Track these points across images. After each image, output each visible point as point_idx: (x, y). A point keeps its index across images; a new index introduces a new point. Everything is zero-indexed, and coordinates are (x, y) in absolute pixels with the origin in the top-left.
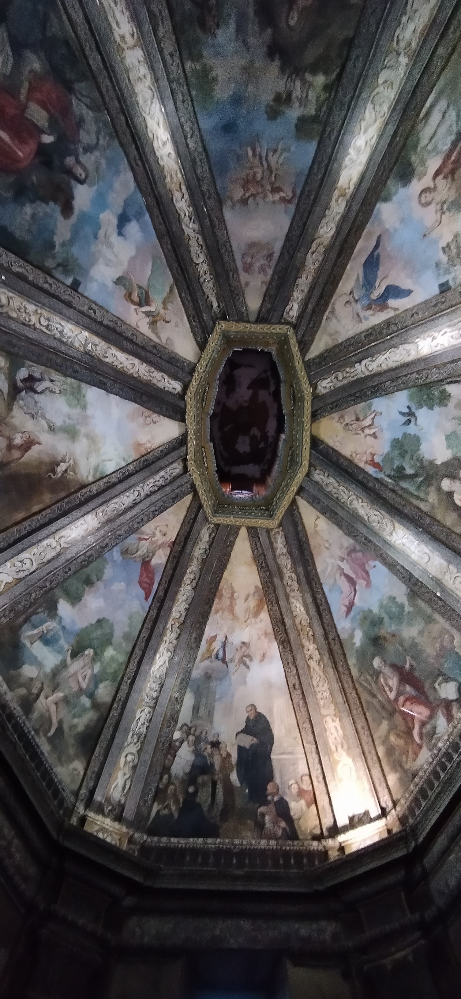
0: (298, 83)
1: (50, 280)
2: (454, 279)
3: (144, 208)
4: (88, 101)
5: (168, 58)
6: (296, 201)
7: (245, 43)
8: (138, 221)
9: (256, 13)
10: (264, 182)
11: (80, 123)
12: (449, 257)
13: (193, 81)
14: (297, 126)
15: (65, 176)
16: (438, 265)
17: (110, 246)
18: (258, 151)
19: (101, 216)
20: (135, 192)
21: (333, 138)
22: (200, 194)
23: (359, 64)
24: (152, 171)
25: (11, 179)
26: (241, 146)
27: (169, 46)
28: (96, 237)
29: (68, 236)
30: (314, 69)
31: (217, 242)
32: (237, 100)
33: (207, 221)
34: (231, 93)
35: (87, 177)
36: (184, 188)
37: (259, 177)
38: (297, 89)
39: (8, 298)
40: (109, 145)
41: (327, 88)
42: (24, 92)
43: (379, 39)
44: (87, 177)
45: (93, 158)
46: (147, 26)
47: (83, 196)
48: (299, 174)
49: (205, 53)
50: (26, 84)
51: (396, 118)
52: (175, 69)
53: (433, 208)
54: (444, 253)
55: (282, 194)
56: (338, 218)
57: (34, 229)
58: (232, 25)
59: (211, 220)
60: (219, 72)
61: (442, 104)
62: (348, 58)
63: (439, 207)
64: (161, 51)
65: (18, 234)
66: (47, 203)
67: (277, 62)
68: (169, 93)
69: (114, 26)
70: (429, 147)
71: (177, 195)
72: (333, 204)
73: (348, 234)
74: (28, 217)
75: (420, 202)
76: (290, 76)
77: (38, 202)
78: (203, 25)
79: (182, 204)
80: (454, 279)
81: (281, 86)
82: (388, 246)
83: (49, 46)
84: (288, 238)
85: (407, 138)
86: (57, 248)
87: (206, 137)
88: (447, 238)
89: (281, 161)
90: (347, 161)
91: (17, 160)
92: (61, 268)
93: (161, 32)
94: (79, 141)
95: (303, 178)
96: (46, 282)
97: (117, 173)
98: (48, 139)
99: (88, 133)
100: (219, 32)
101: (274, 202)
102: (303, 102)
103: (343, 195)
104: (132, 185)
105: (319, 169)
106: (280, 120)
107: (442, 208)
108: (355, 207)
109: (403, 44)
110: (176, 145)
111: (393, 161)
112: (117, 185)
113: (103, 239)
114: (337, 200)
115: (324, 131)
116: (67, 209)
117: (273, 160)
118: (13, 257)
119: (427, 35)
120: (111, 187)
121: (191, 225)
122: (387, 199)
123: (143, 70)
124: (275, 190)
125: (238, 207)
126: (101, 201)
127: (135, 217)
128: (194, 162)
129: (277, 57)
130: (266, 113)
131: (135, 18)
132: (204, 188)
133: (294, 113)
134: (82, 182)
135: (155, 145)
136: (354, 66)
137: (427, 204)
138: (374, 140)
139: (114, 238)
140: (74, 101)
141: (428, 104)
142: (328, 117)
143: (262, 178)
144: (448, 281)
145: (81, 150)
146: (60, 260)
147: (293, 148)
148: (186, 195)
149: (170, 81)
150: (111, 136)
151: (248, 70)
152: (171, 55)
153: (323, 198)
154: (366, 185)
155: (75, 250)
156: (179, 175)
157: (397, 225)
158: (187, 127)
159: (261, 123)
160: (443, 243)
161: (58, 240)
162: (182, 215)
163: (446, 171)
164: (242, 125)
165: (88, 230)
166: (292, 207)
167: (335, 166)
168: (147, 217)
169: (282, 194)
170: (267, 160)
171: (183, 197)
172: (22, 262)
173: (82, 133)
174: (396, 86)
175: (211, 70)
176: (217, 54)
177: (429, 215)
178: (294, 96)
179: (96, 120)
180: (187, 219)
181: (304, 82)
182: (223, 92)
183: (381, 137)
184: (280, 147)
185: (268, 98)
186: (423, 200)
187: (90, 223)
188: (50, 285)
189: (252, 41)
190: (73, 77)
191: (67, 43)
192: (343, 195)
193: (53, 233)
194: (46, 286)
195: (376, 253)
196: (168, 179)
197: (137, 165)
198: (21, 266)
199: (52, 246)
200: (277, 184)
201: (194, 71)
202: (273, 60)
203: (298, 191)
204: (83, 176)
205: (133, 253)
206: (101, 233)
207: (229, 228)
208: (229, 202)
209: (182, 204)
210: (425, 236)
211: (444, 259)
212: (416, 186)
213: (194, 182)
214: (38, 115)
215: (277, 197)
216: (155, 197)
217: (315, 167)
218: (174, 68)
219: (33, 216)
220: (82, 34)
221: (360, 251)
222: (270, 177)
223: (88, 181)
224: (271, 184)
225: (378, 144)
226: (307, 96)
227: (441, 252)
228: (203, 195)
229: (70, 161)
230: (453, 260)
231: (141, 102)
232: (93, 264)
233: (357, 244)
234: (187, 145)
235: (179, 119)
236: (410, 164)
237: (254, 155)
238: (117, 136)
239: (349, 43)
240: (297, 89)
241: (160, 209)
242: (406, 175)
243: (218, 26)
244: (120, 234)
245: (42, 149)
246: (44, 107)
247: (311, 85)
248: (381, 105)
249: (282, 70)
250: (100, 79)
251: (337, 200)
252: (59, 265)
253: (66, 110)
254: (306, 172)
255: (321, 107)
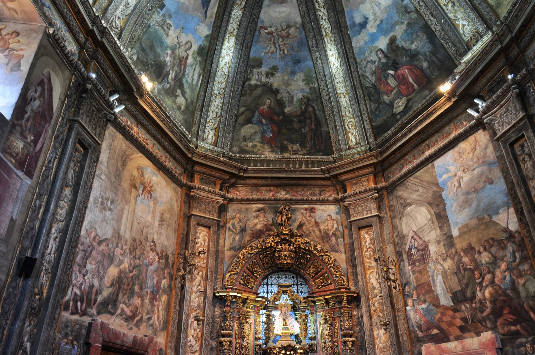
0: (263, 80)
1: (418, 6)
2: (159, 13)
3: (349, 28)
4: (367, 79)
5: (325, 88)
6: (258, 28)
7: (289, 94)
8: (354, 22)
9: (285, 103)
10: (277, 37)
11: (373, 73)
12: (167, 23)
13: (314, 80)
14: (262, 64)
15: (388, 55)
16: (170, 17)
17: (374, 14)
18: (281, 53)
19: (375, 31)
20: (353, 37)
21: (242, 59)
22: (315, 32)
23: (236, 89)
24: (341, 45)
25: (416, 63)
26: (291, 54)
27: (324, 93)
28: (382, 21)
29: (397, 27)
30: (256, 86)
31: (306, 4)
32: (293, 73)
33: (312, 17)
34: (296, 76)
35: (377, 51)
36: (324, 34)
37: (281, 40)
38: (264, 79)
39: (447, 5)
40: (362, 60)
41: (249, 79)
42: (395, 91)
43: (230, 98)
44: (377, 51)
45: (372, 58)
46: (333, 100)
47: (383, 43)
48: (257, 42)
49: (308, 90)
50: (392, 93)
51: (213, 72)
52: (323, 84)
53: (184, 42)
54: (170, 24)
55: (266, 31)
56: (231, 21)
57: (414, 36)
58: (295, 99)
59: (309, 17)
60: (301, 84)
61: (194, 82)
62: (242, 90)
63: (181, 44)
64: (328, 91)
65: (424, 37)
66: (403, 46)
67: (274, 88)
68: (327, 77)
69: (348, 101)
70: (194, 65)
71: (328, 31)
72: (236, 28)
73: (223, 16)
74: (415, 43)
75: (191, 42)
76: (268, 83)
77: (407, 48)
78: (308, 99)
79: (326, 26)
80: (159, 13)
81: (272, 80)
82: (200, 15)
83: (379, 101)
84: (260, 7)
85: (205, 65)
86: (406, 22)
87: (310, 58)
88: (171, 32)
89: (269, 48)
90: (232, 49)
91: (409, 69)
92: (409, 10)
93: (327, 97)
94: (376, 67)
95: (255, 39)
96: (420, 6)
97: (360, 48)
98: (392, 72)
99: (371, 68)
100: (301, 97)
101: (271, 27)
102: (260, 74)
103: (230, 33)
104: (354, 40)
105: (247, 45)
106: (271, 66)
107: (179, 44)
108: (223, 28)
109: (219, 97)
110: (326, 55)
111: (209, 54)
112: (362, 42)
113: (378, 19)
114: (234, 30)
115: (247, 62)
116: (393, 41)
117: (273, 48)
118: (433, 27)
119: (210, 102)
120: (366, 43)
121: (322, 14)
122: (207, 36)
123: (338, 85)
124: (271, 33)
125: (292, 24)
126: (373, 38)
127: (356, 25)
128: (317, 46)
129: (274, 90)
130: (278, 69)
131: (338, 103)
132: (312, 34)
133: (264, 69)
134: (381, 50)
135: (337, 55)
136: (238, 88)
137: (187, 43)
138: (221, 59)
139: (371, 17)
140: (373, 81)
141: (200, 80)
142: (246, 68)
143: (279, 39)
144: (161, 10)
145: (377, 63)
146: (407, 15)
147: (263, 54)
148: (323, 30)
149: (326, 80)
150: (360, 64)
151: (287, 84)
152: (324, 89)
153: (242, 31)
154: (220, 40)
155: (396, 18)
156: (326, 40)
157: (198, 27)
158: (319, 62)
159: (281, 64)
160: (172, 28)
161: (404, 27)
162: (327, 20)
163: (184, 60)
164: (291, 63)
165: (385, 26)
166: (260, 24)
167: (238, 47)
168: (348, 23)
169: (266, 31)
170: (277, 48)
171: (325, 29)
172: (429, 23)
173: (374, 69)
174: (216, 83)
175: (305, 84)
176: (302, 90)
177: (184, 39)
178: (265, 76)
179: (365, 72)
180: (324, 17)
181: (261, 81)
182: (300, 76)
183: (218, 62)
184: (270, 55)
185: (278, 75)
186: (189, 44)
187: (382, 29)
188: (419, 3)
189: (286, 95)
190: (371, 89)
191: (370, 100)
192: (230, 33)
193: (405, 31)
194: (421, 3)
195: (205, 9)
196: (333, 39)
197: (349, 49)
198: (431, 21)
199: (409, 24)
200: (270, 36)
201: (313, 83)
202: (276, 88)
203: (257, 33)
204: (379, 52)
205: (361, 6)
206: (378, 22)
207: (298, 11)
208: (298, 26)
209: (326, 26)
210: (183, 28)
211: (168, 21)
212: (195, 48)
213: (318, 37)
214: (392, 82)
215: (269, 30)
216: (341, 32)
217: (249, 46)
218: (323, 85)
219: (412, 43)
220: (363, 101)
221: (215, 5)
222: (274, 40)
223: (377, 49)
224: (274, 37)
225: (219, 59)
226: (258, 76)
227: (171, 24)
228: (313, 29)
229: (384, 60)
230: (164, 22)
231: (341, 74)
232: (388, 7)
233: (218, 10)
234: (320, 54)
235: (322, 66)
236: (200, 56)
237: (284, 50)
238: (356, 63)
239: (242, 95)
240: (264, 79)
241: (340, 25)
242: (201, 51)
243: (302, 99)
244: (367, 19)
245: (396, 69)
246: (388, 84)
247: (257, 80)
248: (221, 74)
249: (271, 85)
250: (359, 86)
251: (234, 30)
252: (409, 13)
253: (379, 79)
254: (254, 43)
255: (250, 72)
